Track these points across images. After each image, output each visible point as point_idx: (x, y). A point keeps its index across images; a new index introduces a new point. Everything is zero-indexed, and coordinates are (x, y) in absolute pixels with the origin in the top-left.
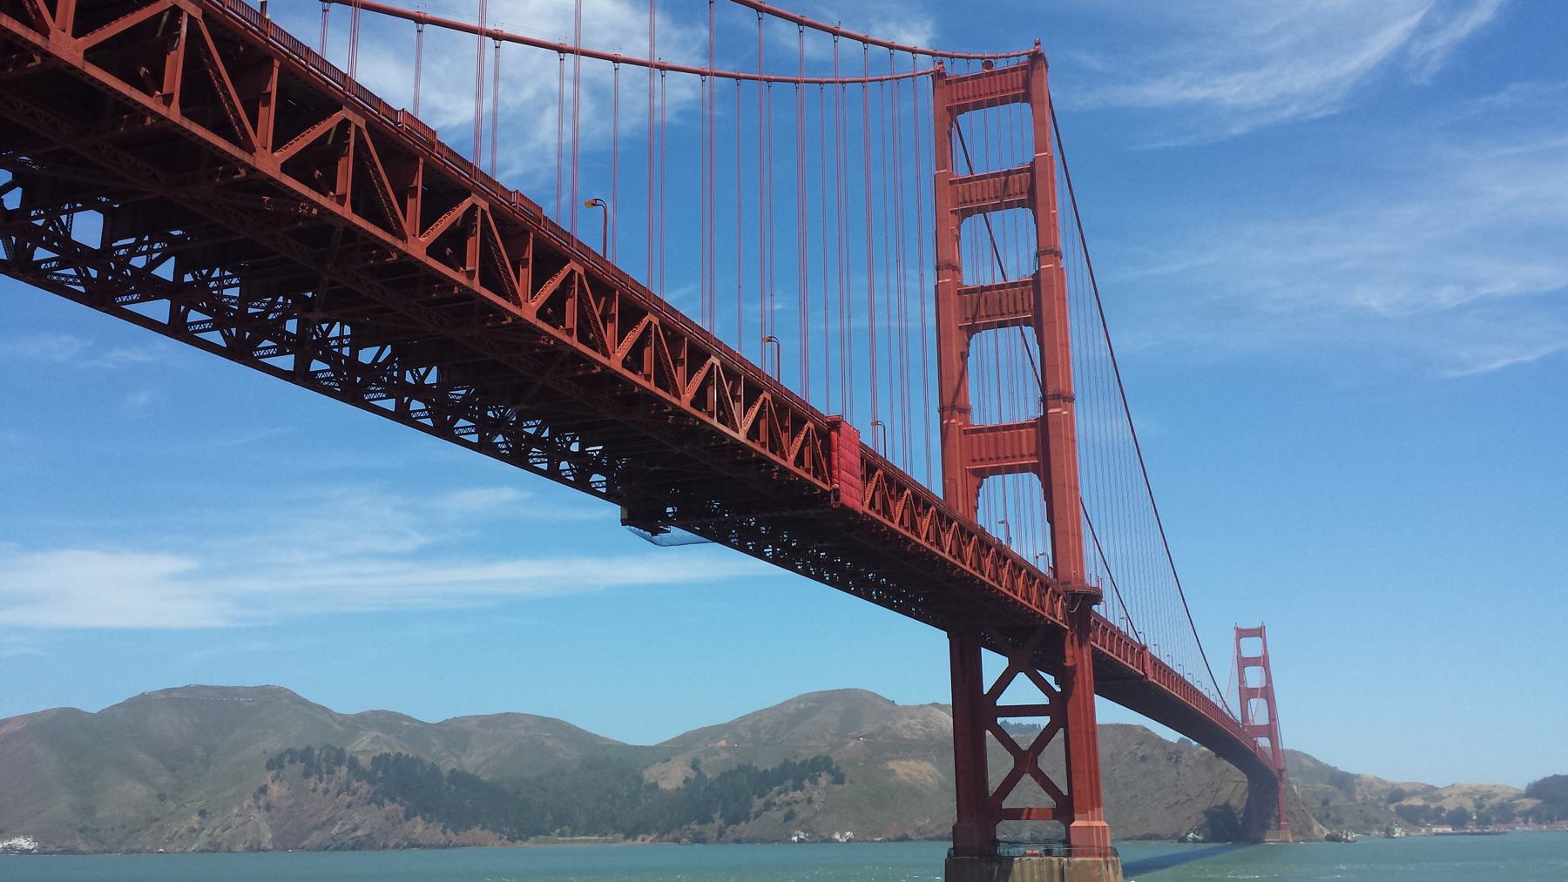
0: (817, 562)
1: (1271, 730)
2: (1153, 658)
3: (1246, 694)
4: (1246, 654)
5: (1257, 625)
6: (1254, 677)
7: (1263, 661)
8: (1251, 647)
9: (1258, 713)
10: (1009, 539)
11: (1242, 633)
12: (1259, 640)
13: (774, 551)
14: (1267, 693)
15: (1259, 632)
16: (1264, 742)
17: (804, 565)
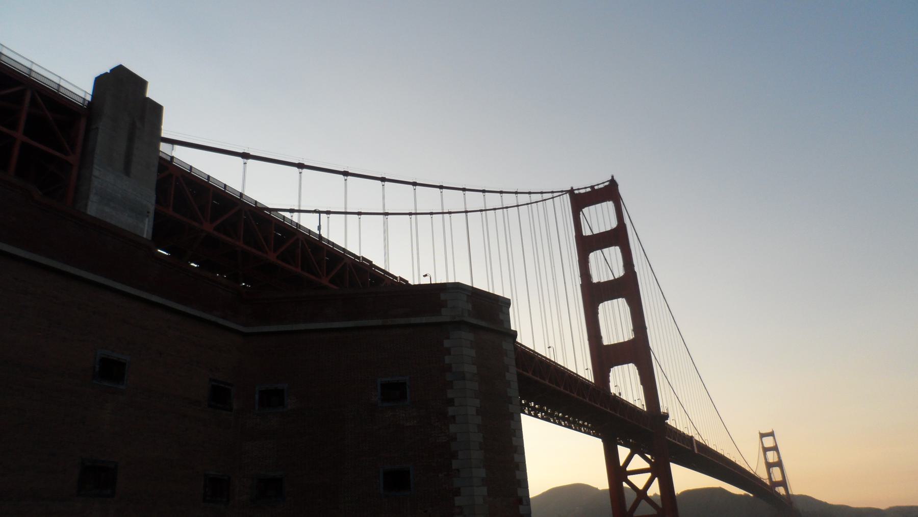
0: (558, 418)
1: (783, 483)
2: (696, 441)
3: (769, 466)
4: (766, 446)
5: (769, 431)
6: (772, 457)
7: (775, 448)
8: (769, 442)
9: (777, 475)
10: (620, 394)
11: (762, 436)
12: (771, 438)
13: (542, 415)
14: (779, 464)
15: (771, 434)
16: (781, 490)
17: (554, 420)
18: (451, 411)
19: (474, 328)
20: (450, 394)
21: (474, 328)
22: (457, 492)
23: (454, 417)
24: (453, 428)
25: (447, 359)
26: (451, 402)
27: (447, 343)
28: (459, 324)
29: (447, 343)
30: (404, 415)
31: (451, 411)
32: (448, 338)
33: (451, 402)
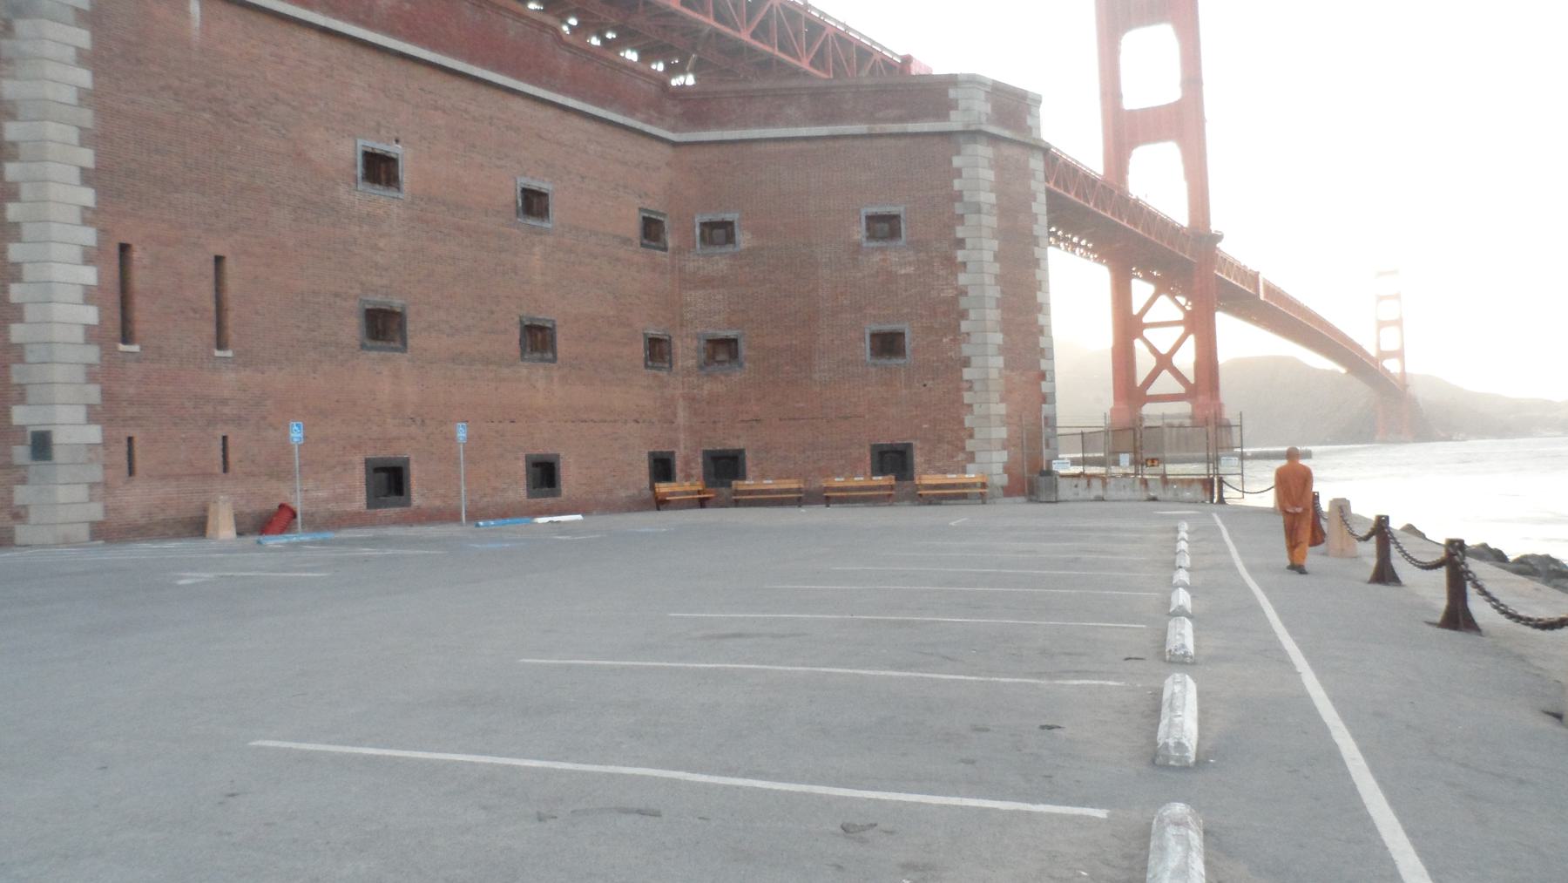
18: (960, 255)
19: (994, 139)
20: (960, 232)
21: (994, 139)
22: (966, 362)
23: (964, 264)
24: (963, 279)
25: (957, 184)
26: (960, 243)
27: (957, 161)
28: (973, 135)
29: (957, 161)
30: (897, 259)
31: (960, 255)
32: (958, 153)
33: (960, 243)
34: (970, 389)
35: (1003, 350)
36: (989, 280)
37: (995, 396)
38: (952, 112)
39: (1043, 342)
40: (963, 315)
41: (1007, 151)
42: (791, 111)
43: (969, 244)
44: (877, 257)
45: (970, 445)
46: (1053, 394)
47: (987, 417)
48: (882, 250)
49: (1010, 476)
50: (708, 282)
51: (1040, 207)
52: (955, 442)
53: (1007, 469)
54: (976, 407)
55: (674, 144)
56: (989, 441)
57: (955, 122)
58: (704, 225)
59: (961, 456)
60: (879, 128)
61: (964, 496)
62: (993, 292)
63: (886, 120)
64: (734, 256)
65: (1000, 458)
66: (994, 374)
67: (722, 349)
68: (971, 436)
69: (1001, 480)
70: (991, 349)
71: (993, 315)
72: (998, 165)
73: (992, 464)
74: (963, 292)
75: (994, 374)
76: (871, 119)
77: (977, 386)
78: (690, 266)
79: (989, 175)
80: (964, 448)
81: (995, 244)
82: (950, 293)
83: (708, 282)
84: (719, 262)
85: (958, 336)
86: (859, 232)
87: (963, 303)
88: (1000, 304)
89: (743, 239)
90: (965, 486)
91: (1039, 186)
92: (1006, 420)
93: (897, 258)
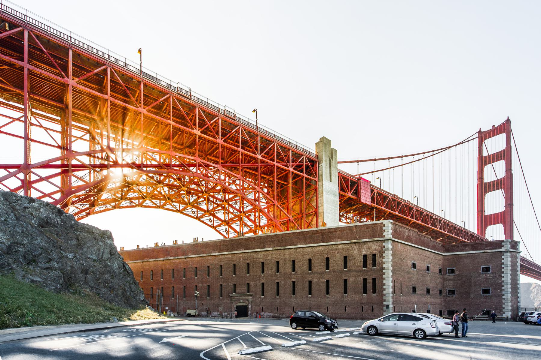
19: (511, 252)
20: (503, 270)
22: (503, 295)
23: (504, 276)
24: (503, 279)
26: (503, 272)
28: (506, 252)
31: (503, 275)
32: (503, 255)
33: (503, 272)
34: (504, 300)
35: (511, 292)
36: (509, 279)
37: (509, 301)
38: (502, 247)
39: (518, 291)
40: (503, 286)
41: (513, 254)
42: (467, 248)
43: (505, 273)
44: (484, 275)
45: (503, 310)
46: (520, 301)
47: (508, 305)
48: (485, 274)
49: (512, 316)
50: (449, 280)
51: (519, 264)
52: (501, 309)
53: (511, 315)
54: (505, 303)
55: (443, 255)
56: (508, 310)
57: (503, 249)
58: (448, 270)
59: (501, 312)
60: (486, 251)
61: (502, 320)
62: (510, 281)
63: (487, 250)
64: (454, 275)
65: (510, 313)
66: (509, 297)
67: (452, 292)
68: (504, 309)
69: (510, 317)
70: (509, 292)
71: (509, 286)
72: (511, 257)
73: (508, 314)
74: (503, 282)
75: (509, 297)
76: (484, 249)
77: (505, 299)
78: (446, 277)
79: (509, 259)
80: (502, 311)
81: (510, 272)
82: (500, 282)
83: (449, 280)
84: (452, 276)
85: (502, 290)
86: (481, 271)
87: (503, 284)
88: (511, 284)
89: (457, 272)
90: (502, 318)
91: (518, 260)
92: (512, 306)
93: (489, 275)
